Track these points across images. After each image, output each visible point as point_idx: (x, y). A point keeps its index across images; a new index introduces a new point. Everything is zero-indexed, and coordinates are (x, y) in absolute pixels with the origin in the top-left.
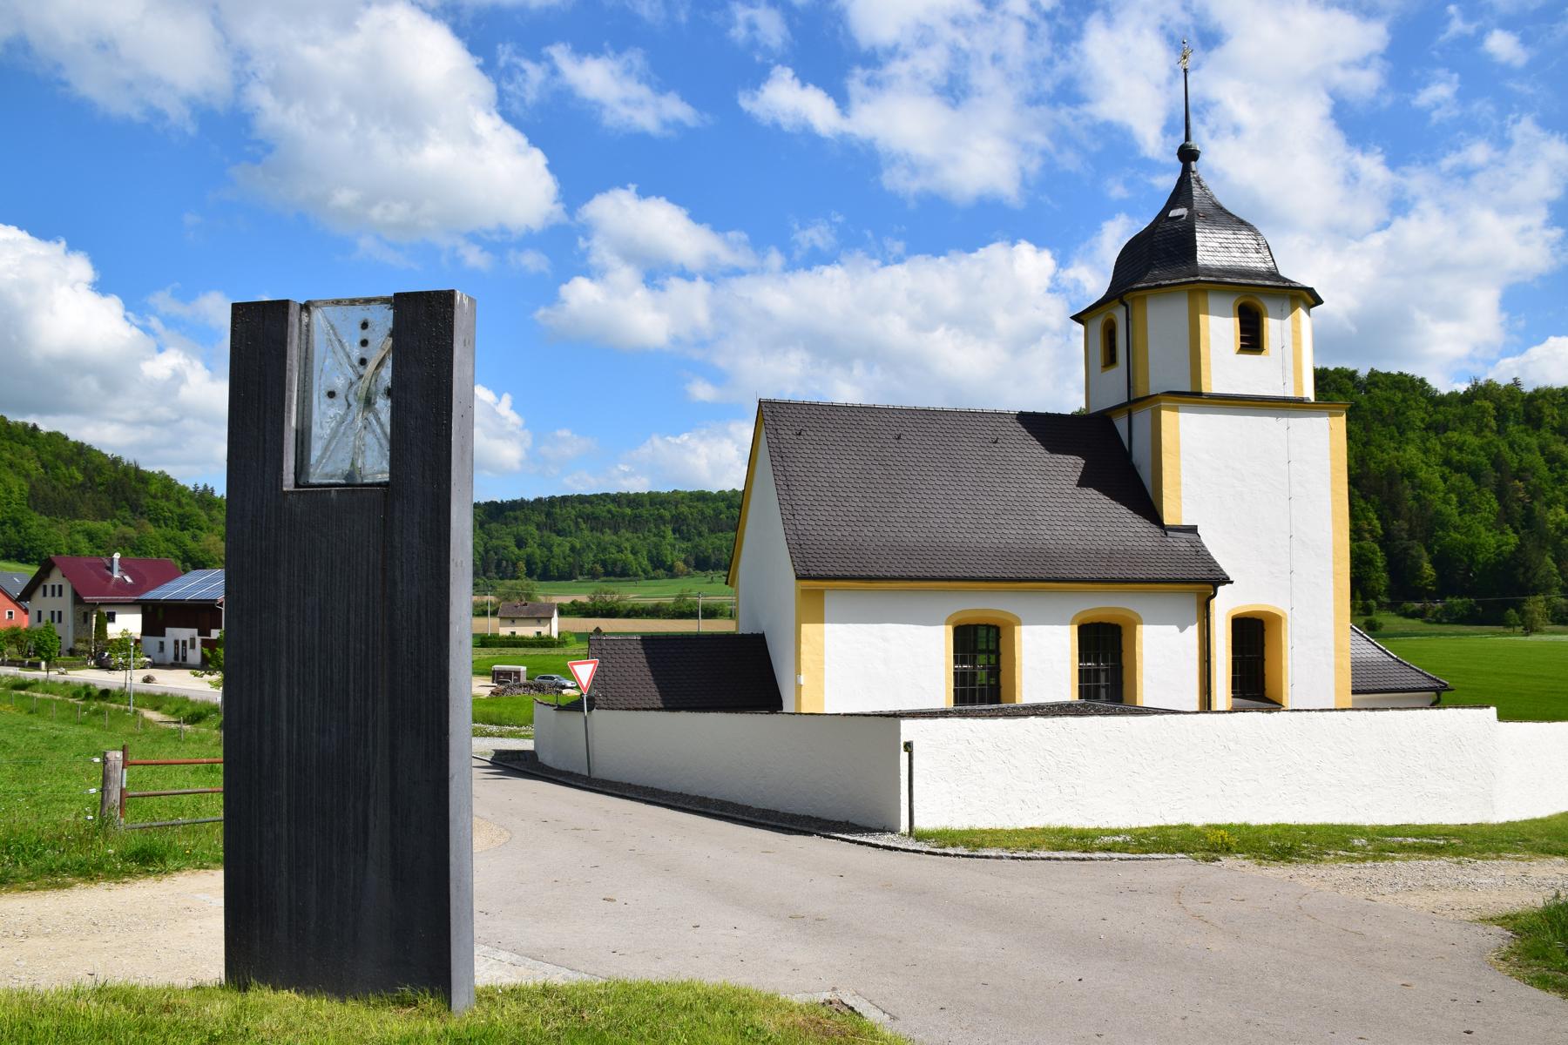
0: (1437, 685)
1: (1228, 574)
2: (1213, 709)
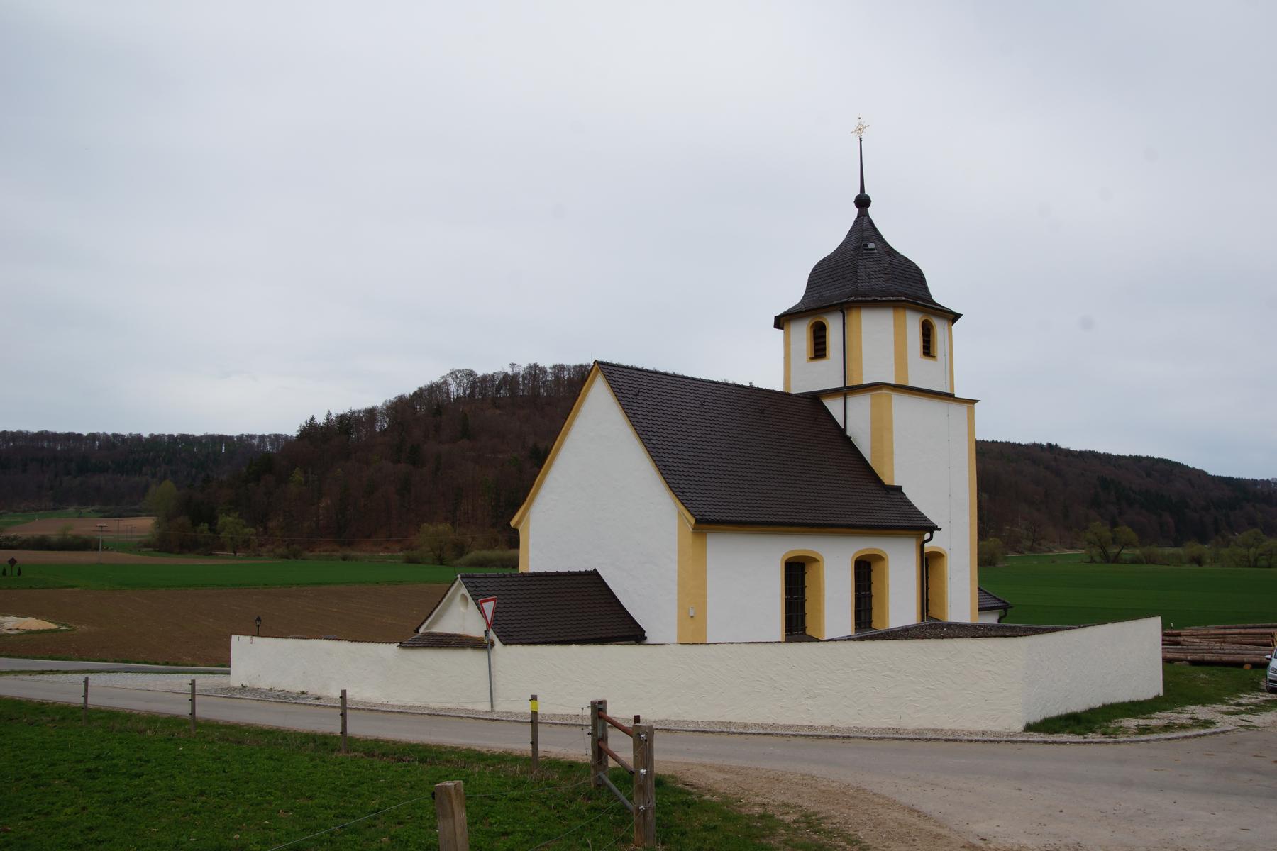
0: (1004, 604)
2: (878, 625)
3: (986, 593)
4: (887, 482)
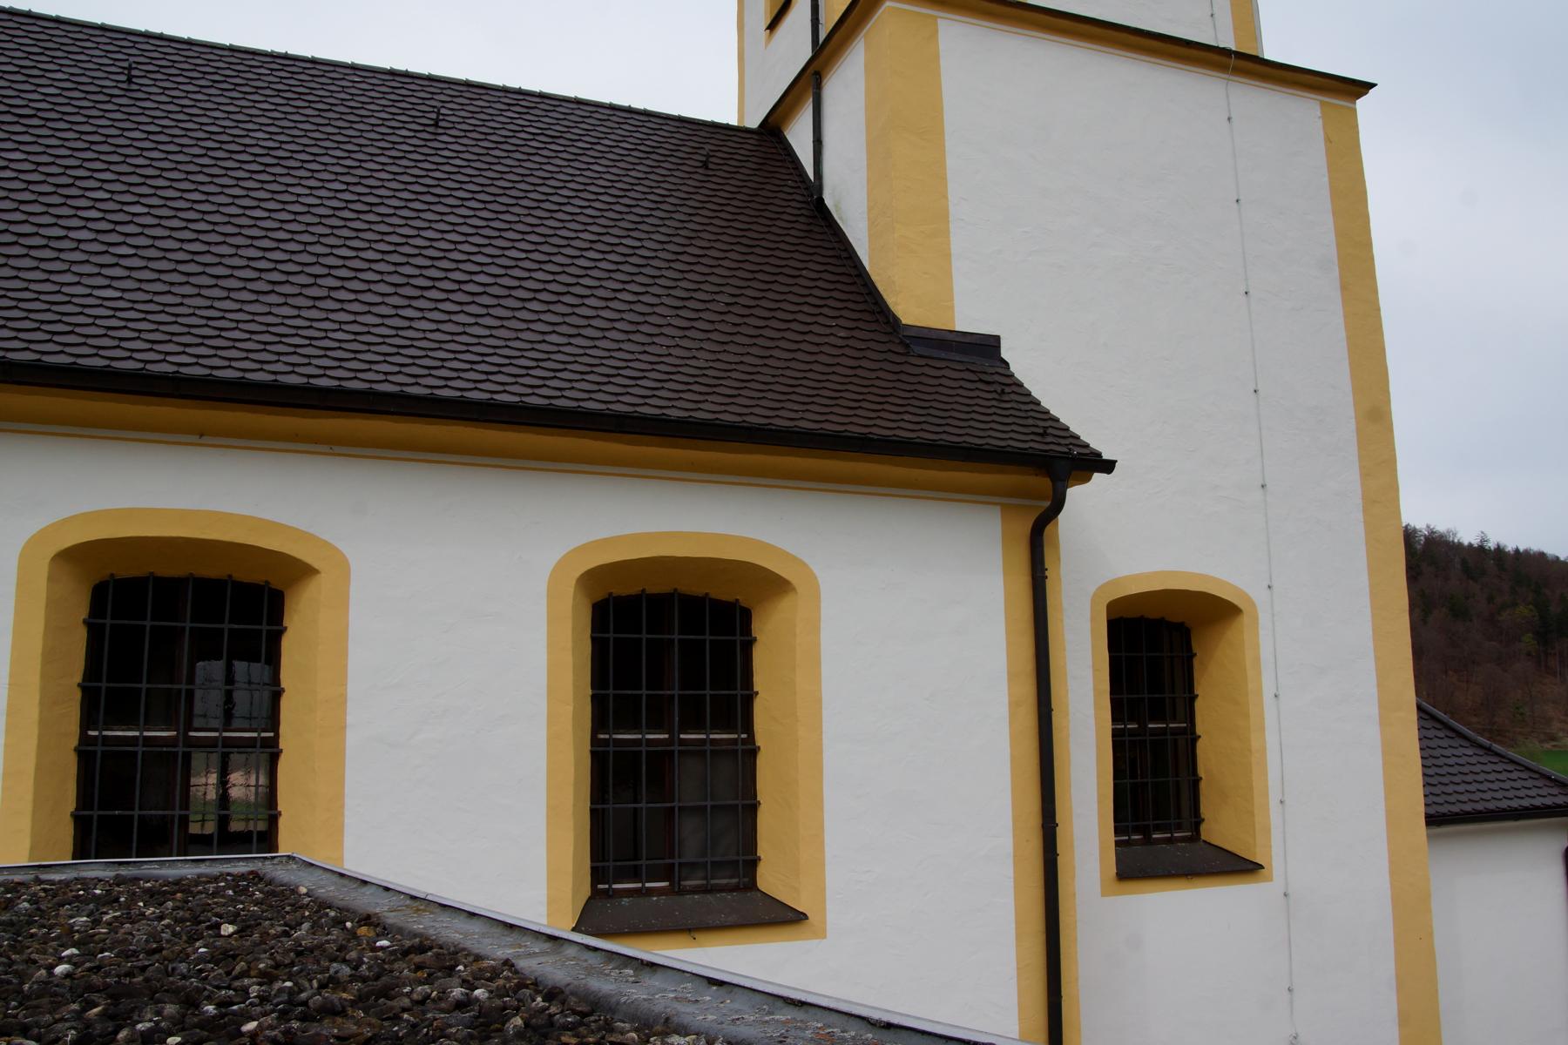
1: (1095, 445)
3: (1512, 761)
4: (910, 309)
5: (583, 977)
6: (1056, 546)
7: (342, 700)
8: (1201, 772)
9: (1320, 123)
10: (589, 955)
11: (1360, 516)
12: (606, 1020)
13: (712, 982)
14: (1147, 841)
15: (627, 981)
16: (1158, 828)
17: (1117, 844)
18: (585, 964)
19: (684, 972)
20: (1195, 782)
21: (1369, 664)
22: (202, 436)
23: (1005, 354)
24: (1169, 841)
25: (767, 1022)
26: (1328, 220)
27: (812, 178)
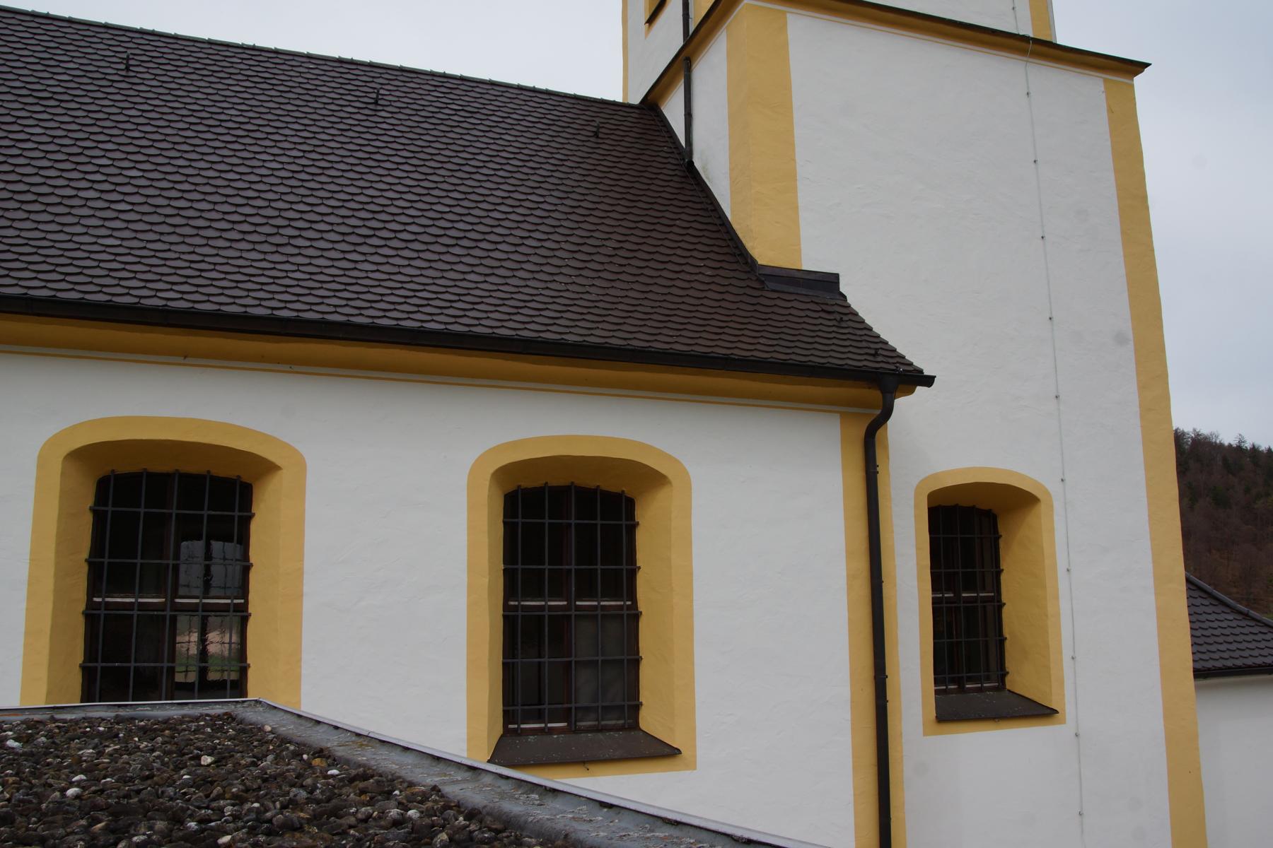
4: (765, 252)
5: (497, 800)
6: (886, 448)
7: (300, 573)
8: (1006, 632)
9: (1103, 96)
10: (502, 782)
11: (1138, 421)
12: (516, 836)
13: (603, 805)
14: (961, 690)
15: (533, 804)
16: (970, 680)
17: (937, 692)
18: (499, 790)
19: (580, 796)
20: (1001, 641)
21: (1146, 544)
22: (186, 357)
23: (843, 289)
24: (980, 690)
25: (648, 838)
26: (1110, 177)
27: (684, 145)
